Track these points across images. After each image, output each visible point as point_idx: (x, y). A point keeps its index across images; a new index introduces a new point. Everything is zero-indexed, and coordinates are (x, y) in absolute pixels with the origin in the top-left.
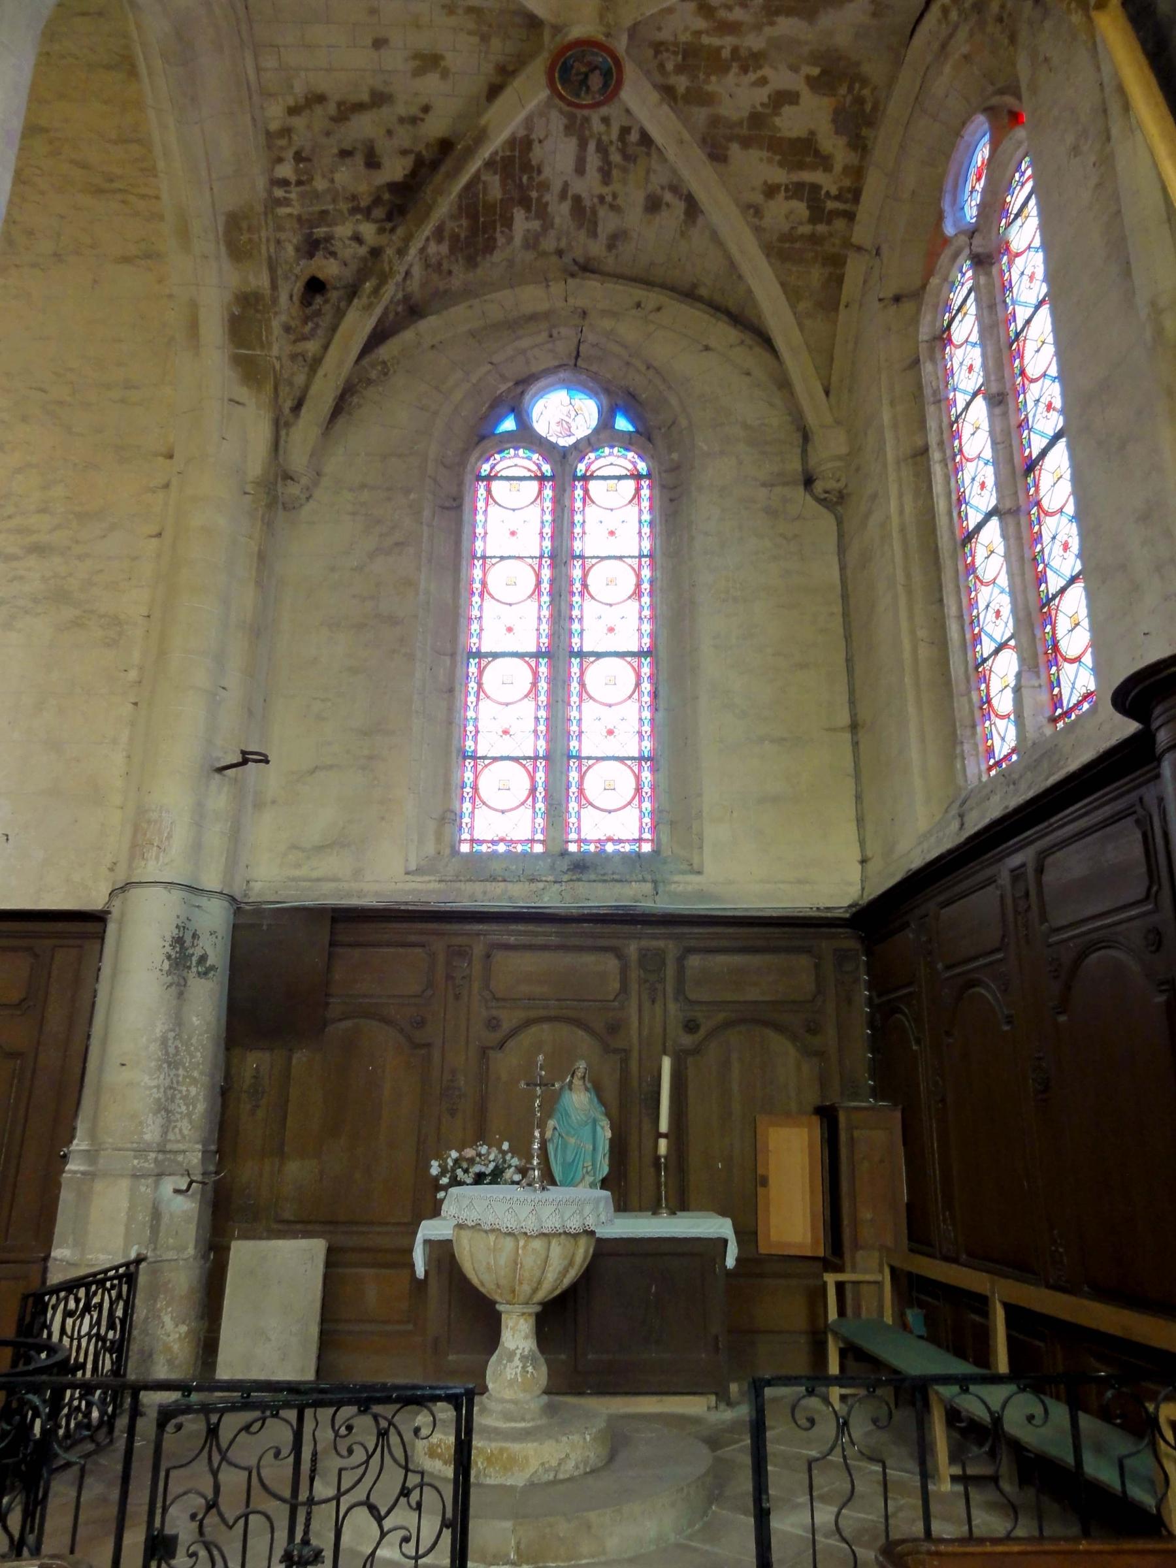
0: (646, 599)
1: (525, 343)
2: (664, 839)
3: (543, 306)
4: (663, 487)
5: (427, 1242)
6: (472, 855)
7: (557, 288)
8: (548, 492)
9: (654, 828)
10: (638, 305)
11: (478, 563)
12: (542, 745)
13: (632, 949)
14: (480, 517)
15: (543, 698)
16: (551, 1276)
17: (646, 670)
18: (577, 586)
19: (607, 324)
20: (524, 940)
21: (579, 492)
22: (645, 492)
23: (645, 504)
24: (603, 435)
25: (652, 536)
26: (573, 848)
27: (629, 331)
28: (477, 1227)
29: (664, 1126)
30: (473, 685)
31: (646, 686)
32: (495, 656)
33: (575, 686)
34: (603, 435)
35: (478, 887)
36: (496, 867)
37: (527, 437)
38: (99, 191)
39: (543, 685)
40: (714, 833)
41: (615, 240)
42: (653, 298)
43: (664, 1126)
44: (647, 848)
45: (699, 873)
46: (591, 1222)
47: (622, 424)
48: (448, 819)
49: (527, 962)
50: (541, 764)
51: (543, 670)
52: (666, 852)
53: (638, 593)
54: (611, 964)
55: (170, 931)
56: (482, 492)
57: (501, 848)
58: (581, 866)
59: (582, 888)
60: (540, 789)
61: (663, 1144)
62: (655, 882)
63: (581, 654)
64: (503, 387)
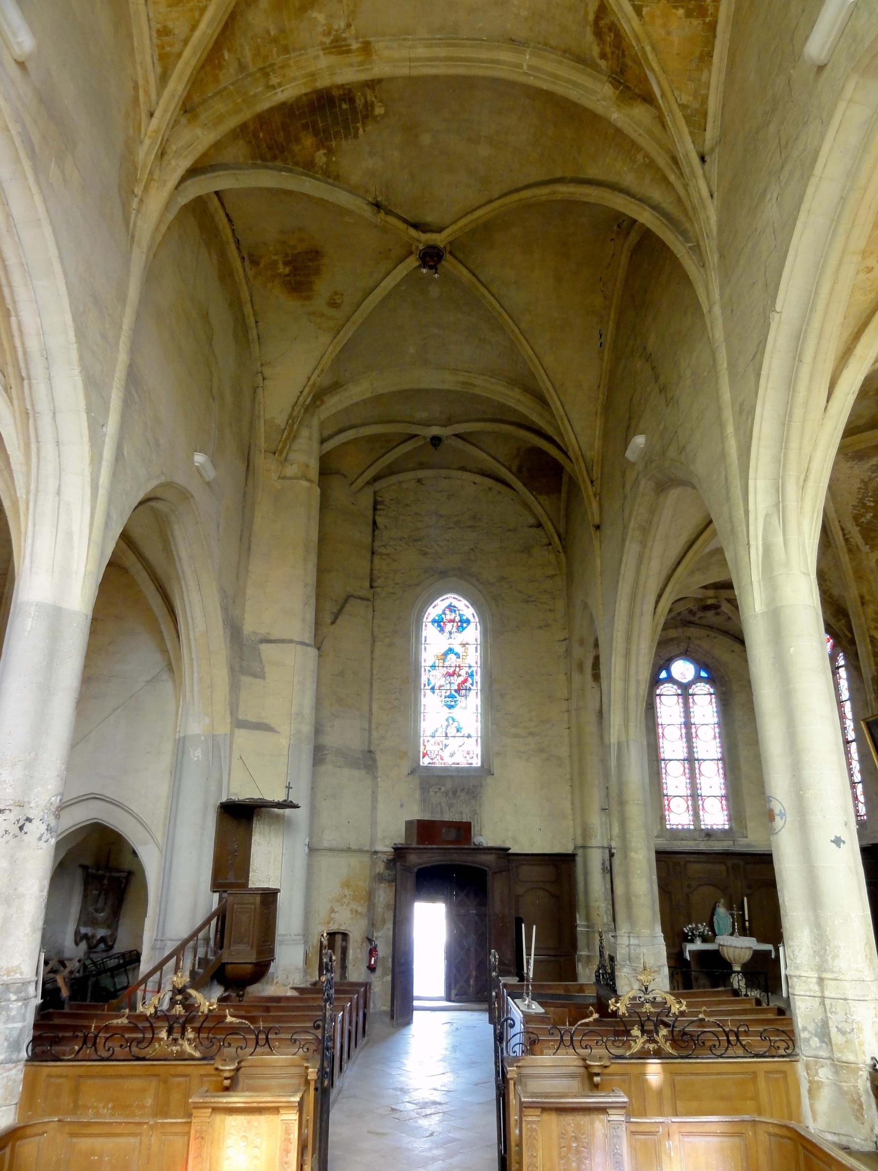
0: (718, 740)
1: (669, 649)
2: (733, 825)
3: (674, 636)
4: (721, 700)
5: (689, 951)
6: (672, 829)
7: (680, 630)
8: (681, 700)
9: (729, 820)
10: (708, 636)
11: (660, 727)
12: (689, 792)
13: (729, 864)
14: (658, 710)
15: (687, 775)
16: (747, 957)
17: (720, 765)
18: (694, 735)
19: (698, 642)
20: (696, 859)
21: (691, 700)
22: (714, 700)
23: (714, 705)
24: (698, 679)
25: (718, 716)
26: (703, 827)
27: (705, 645)
28: (731, 946)
29: (747, 918)
30: (664, 771)
31: (721, 771)
32: (670, 760)
33: (697, 771)
34: (698, 679)
35: (679, 842)
36: (682, 834)
37: (670, 679)
38: (527, 601)
39: (687, 771)
40: (751, 825)
41: (700, 618)
42: (712, 634)
43: (747, 918)
44: (727, 827)
45: (746, 837)
46: (751, 946)
47: (703, 674)
48: (663, 818)
49: (699, 867)
50: (690, 798)
51: (687, 766)
52: (734, 829)
53: (715, 738)
54: (723, 868)
55: (601, 861)
56: (658, 700)
57: (680, 827)
58: (709, 834)
59: (710, 843)
60: (690, 807)
61: (747, 923)
62: (733, 841)
63: (698, 760)
64: (662, 662)
